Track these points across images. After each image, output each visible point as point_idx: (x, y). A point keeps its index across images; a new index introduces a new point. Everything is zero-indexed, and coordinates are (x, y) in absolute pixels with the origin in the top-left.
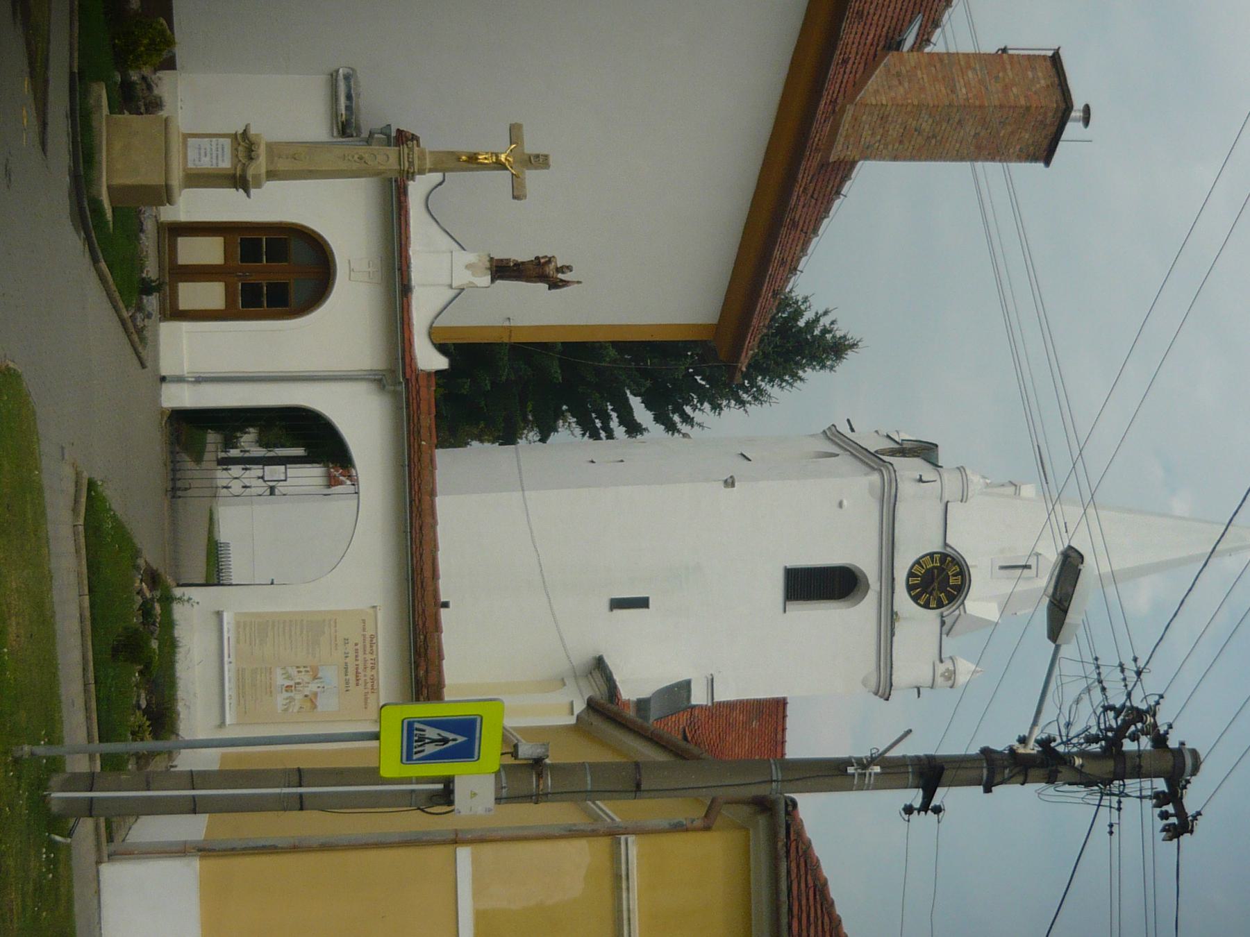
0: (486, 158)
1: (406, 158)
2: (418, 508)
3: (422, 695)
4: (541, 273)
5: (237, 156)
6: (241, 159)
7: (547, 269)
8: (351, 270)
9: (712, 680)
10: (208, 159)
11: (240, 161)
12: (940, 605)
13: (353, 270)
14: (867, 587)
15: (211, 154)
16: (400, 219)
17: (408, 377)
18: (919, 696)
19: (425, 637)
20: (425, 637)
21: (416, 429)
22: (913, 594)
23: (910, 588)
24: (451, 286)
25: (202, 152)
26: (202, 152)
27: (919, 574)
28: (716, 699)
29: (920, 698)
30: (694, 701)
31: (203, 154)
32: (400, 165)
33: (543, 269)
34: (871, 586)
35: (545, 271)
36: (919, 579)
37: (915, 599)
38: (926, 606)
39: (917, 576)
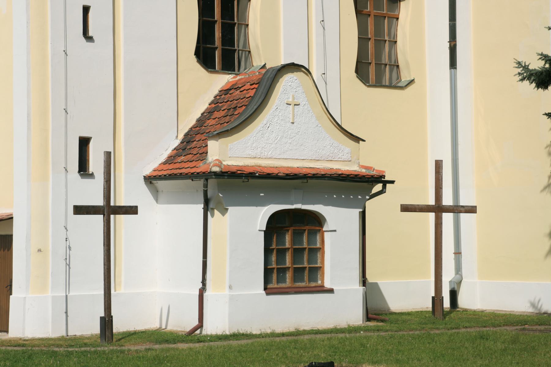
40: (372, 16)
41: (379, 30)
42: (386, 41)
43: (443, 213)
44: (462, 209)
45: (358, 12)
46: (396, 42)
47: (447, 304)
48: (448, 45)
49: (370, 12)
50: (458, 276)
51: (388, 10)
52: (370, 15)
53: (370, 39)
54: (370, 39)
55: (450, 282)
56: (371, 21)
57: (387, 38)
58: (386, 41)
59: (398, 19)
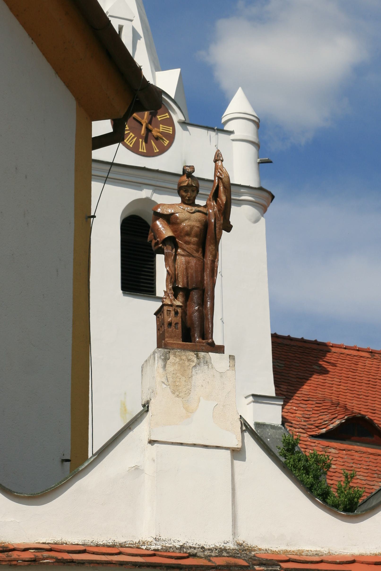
9: (254, 396)
12: (170, 122)
14: (148, 201)
18: (271, 162)
22: (158, 151)
23: (150, 154)
27: (135, 140)
28: (274, 395)
29: (273, 161)
30: (278, 422)
33: (188, 234)
34: (149, 196)
35: (192, 228)
36: (141, 140)
37: (163, 150)
38: (171, 138)
39: (137, 142)
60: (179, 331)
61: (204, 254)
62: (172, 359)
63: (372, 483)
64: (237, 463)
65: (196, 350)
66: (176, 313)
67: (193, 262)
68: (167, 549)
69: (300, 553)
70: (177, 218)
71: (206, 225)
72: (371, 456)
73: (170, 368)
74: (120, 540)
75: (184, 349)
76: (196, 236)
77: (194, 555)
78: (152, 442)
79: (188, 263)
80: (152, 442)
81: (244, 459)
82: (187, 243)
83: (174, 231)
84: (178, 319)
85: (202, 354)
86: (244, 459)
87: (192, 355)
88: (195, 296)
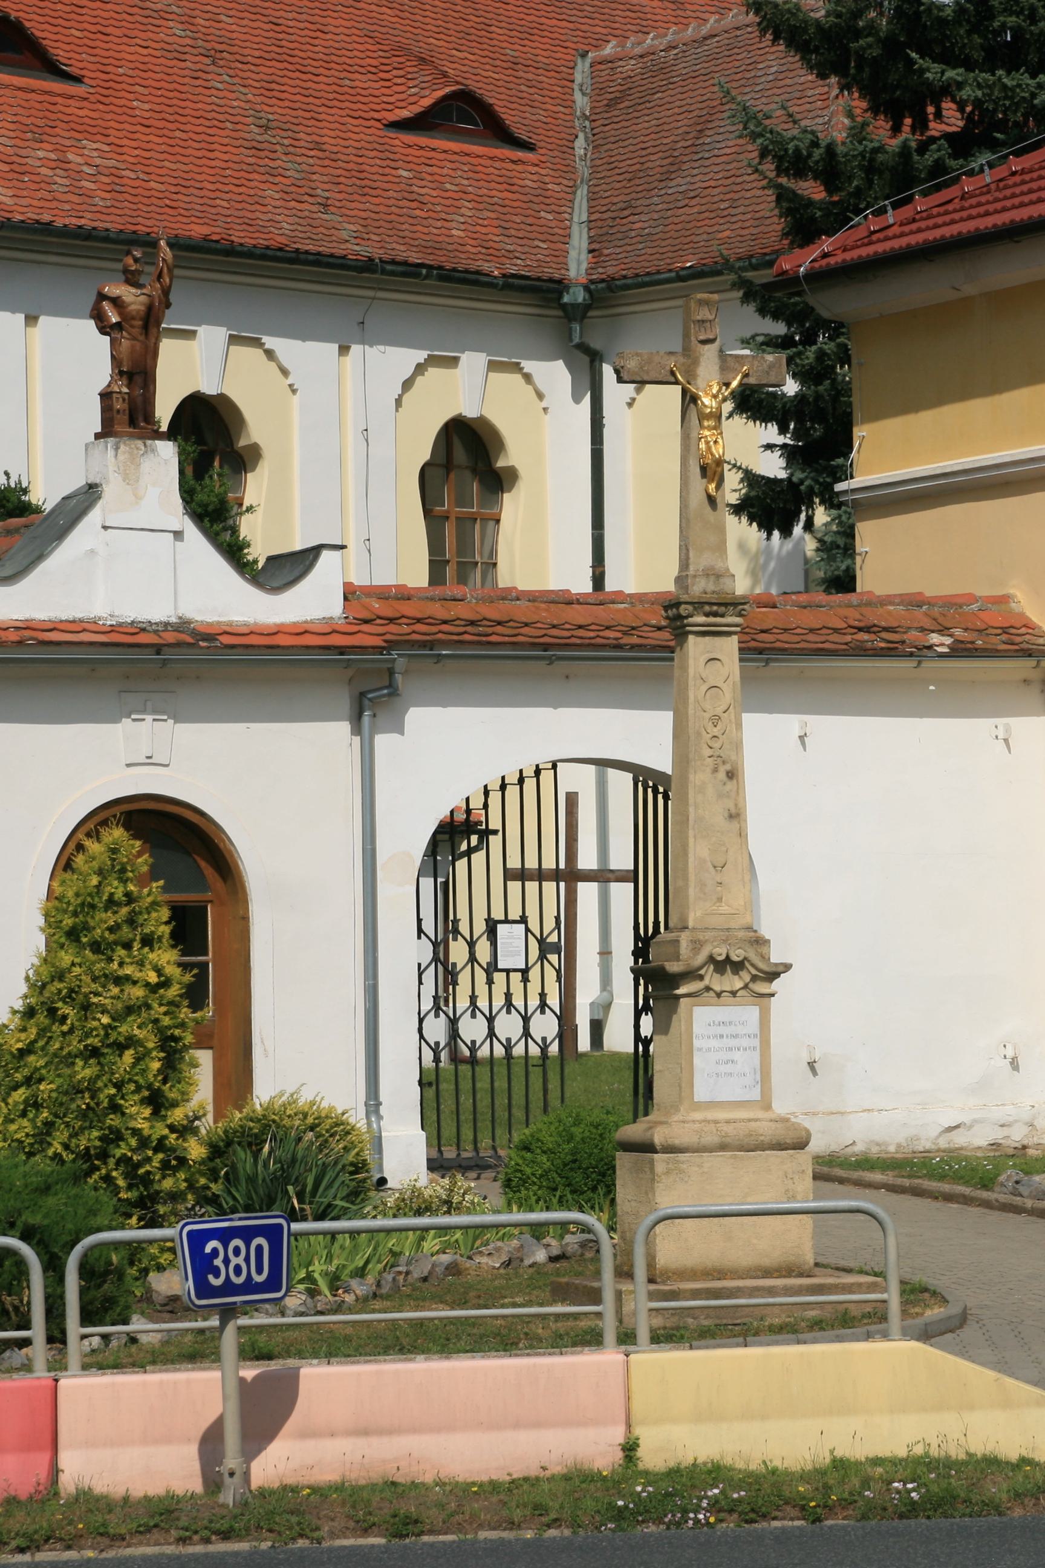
0: (716, 442)
1: (718, 620)
2: (625, 633)
3: (973, 643)
4: (140, 323)
5: (734, 993)
6: (738, 984)
7: (133, 307)
8: (149, 762)
10: (737, 1055)
11: (746, 987)
13: (148, 757)
15: (731, 1049)
16: (58, 644)
17: (378, 642)
19: (860, 629)
20: (860, 629)
21: (469, 629)
24: (178, 535)
25: (723, 1068)
26: (723, 1068)
31: (728, 1068)
32: (729, 634)
33: (133, 318)
35: (138, 311)
40: (453, 519)
41: (464, 544)
42: (477, 563)
43: (579, 884)
44: (610, 876)
45: (427, 513)
46: (495, 564)
47: (584, 1043)
48: (589, 572)
49: (448, 511)
50: (605, 994)
51: (480, 506)
52: (448, 518)
53: (448, 562)
54: (448, 562)
55: (592, 1004)
56: (449, 531)
57: (478, 558)
58: (477, 563)
59: (498, 521)
60: (126, 417)
61: (147, 334)
62: (122, 447)
63: (23, 152)
64: (178, 543)
65: (143, 437)
66: (124, 400)
67: (138, 346)
68: (120, 625)
69: (230, 624)
70: (123, 302)
71: (150, 308)
72: (19, 93)
73: (121, 457)
74: (79, 615)
75: (132, 436)
76: (141, 319)
77: (143, 630)
78: (105, 528)
79: (133, 346)
80: (105, 528)
81: (182, 540)
82: (132, 326)
83: (120, 314)
84: (126, 406)
85: (149, 442)
86: (182, 540)
87: (139, 443)
88: (139, 379)
